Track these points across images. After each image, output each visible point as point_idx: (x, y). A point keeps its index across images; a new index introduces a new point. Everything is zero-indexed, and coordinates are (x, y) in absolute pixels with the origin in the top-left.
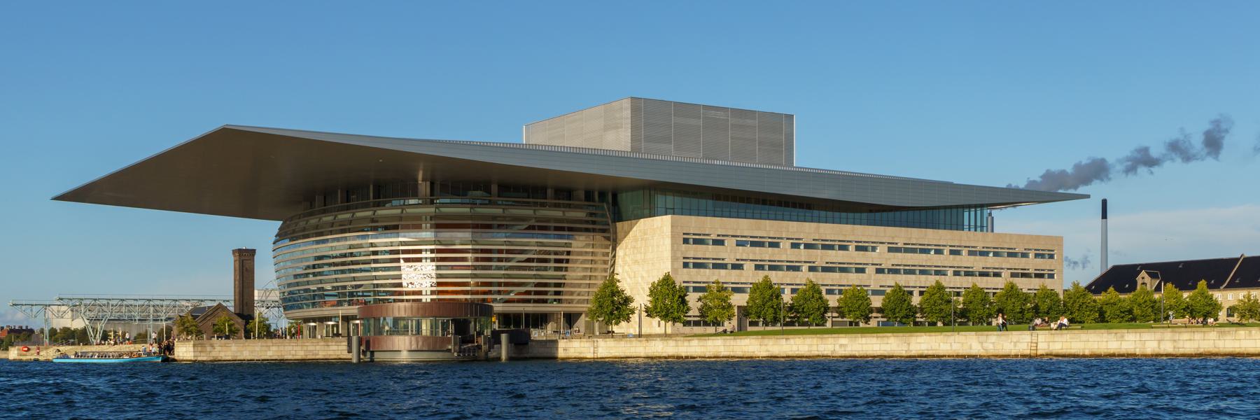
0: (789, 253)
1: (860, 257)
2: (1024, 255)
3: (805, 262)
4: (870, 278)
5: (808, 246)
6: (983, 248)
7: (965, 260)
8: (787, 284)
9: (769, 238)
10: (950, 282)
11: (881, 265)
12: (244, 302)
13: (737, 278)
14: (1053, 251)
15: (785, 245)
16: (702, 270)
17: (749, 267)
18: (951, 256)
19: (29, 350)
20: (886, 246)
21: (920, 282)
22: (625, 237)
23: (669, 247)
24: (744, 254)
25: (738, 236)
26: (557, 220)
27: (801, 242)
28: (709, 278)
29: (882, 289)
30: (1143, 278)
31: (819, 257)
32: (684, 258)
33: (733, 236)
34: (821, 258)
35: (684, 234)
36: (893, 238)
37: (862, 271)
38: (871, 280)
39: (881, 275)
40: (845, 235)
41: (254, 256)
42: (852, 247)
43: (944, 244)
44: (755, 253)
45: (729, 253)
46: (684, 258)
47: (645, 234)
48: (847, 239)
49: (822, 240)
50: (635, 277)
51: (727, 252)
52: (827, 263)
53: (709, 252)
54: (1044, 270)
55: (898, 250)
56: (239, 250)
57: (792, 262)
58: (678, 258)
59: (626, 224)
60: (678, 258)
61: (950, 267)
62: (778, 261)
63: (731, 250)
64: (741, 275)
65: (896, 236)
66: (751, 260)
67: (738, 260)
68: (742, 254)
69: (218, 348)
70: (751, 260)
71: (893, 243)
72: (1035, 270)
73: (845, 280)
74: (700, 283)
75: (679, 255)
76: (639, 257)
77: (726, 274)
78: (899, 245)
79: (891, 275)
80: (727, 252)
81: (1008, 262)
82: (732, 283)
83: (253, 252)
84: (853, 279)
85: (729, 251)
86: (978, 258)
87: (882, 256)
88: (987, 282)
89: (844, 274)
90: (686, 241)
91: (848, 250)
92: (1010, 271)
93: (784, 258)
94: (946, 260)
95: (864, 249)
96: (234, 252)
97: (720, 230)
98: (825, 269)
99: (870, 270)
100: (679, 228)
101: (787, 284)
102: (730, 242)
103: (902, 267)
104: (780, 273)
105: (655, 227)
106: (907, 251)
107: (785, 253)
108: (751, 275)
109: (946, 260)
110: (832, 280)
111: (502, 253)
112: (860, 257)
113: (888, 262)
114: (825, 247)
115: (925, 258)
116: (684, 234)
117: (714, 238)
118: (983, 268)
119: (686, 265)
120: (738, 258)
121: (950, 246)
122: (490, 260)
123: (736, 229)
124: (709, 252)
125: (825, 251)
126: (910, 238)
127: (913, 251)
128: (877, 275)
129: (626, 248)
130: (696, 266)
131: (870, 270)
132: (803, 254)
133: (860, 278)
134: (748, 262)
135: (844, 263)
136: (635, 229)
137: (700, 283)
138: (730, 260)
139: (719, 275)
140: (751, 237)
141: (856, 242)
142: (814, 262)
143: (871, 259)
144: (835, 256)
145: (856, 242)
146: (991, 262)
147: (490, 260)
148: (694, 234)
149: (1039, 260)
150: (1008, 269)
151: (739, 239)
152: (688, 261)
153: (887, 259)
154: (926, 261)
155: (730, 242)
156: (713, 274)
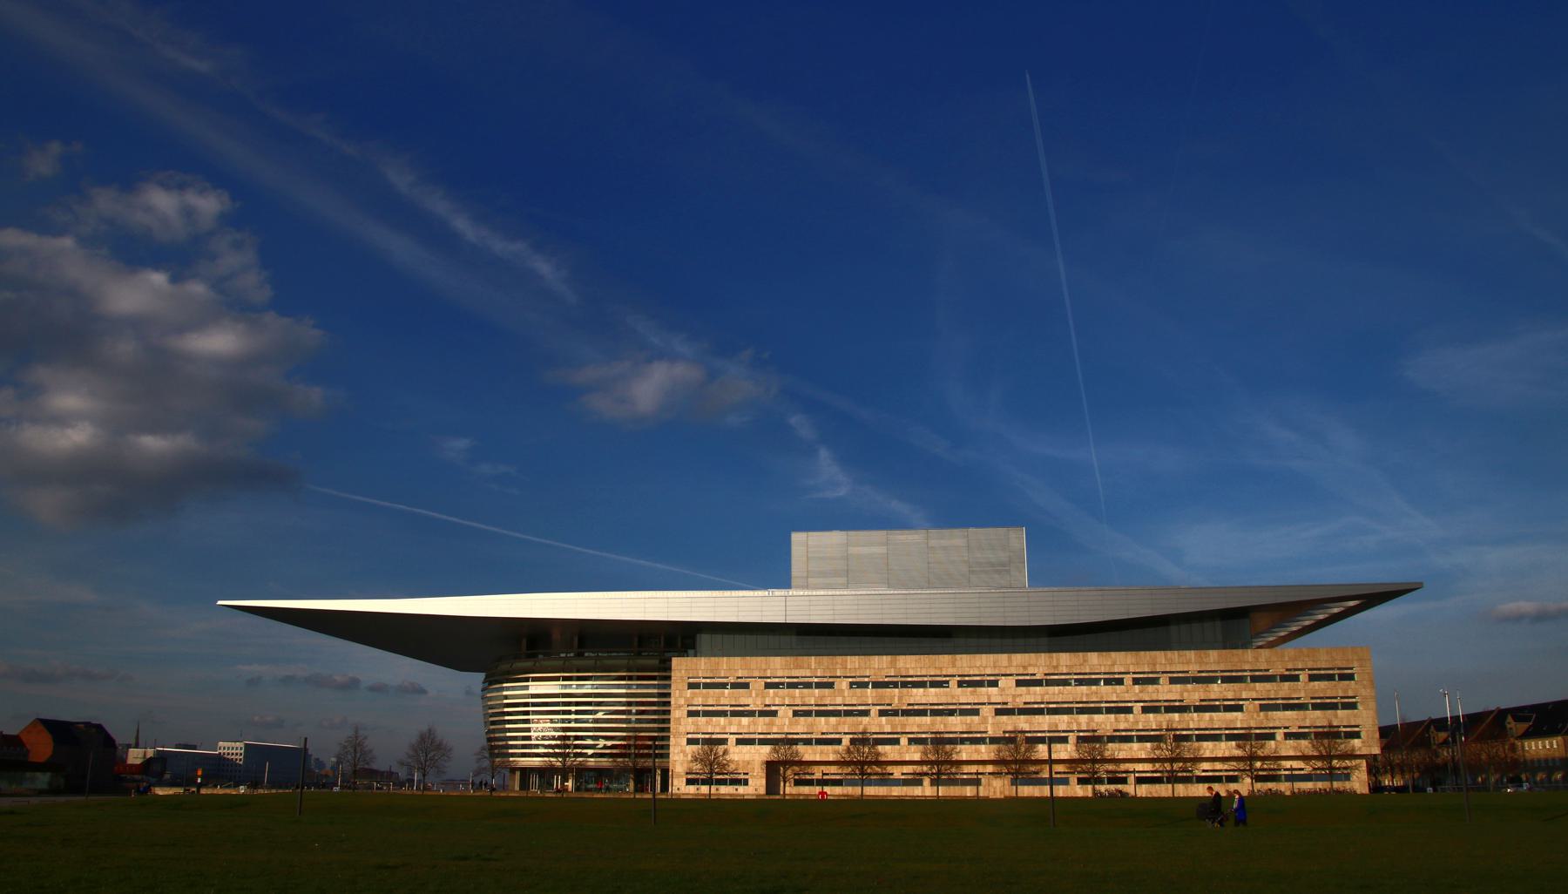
0: (846, 694)
1: (965, 696)
2: (1284, 678)
4: (985, 721)
5: (877, 685)
6: (1199, 672)
7: (1165, 692)
10: (1137, 722)
11: (1006, 703)
13: (765, 727)
14: (1352, 669)
15: (844, 684)
16: (714, 719)
17: (785, 714)
18: (1137, 686)
20: (1011, 681)
21: (1079, 724)
24: (777, 699)
25: (769, 678)
27: (866, 680)
28: (725, 728)
31: (896, 701)
34: (895, 697)
36: (1025, 668)
37: (976, 712)
38: (993, 725)
40: (941, 669)
42: (953, 682)
44: (794, 697)
45: (752, 700)
48: (944, 673)
49: (902, 676)
51: (751, 696)
52: (909, 705)
53: (727, 697)
54: (1336, 698)
55: (1038, 683)
57: (855, 705)
58: (680, 706)
60: (680, 706)
61: (1136, 702)
62: (831, 705)
63: (757, 695)
64: (772, 724)
65: (1030, 665)
66: (788, 705)
67: (766, 705)
68: (774, 698)
70: (788, 705)
71: (1027, 675)
72: (1312, 698)
73: (942, 726)
75: (682, 701)
77: (749, 723)
80: (751, 696)
81: (1254, 689)
84: (956, 724)
85: (754, 695)
86: (1189, 686)
87: (1007, 692)
88: (1211, 719)
89: (939, 718)
90: (692, 686)
92: (1257, 702)
93: (839, 700)
94: (1127, 692)
95: (980, 684)
97: (740, 671)
98: (906, 713)
99: (987, 711)
100: (683, 671)
103: (1042, 706)
104: (833, 720)
106: (1050, 683)
107: (843, 695)
108: (787, 723)
109: (1127, 692)
110: (919, 726)
112: (965, 696)
113: (1018, 700)
114: (905, 685)
115: (1085, 692)
117: (732, 681)
118: (1201, 700)
119: (691, 714)
120: (767, 703)
121: (1134, 673)
122: (569, 712)
123: (765, 670)
124: (727, 697)
125: (905, 690)
126: (1056, 667)
127: (1065, 683)
128: (998, 717)
130: (707, 714)
131: (987, 711)
133: (968, 722)
139: (740, 724)
141: (959, 676)
142: (888, 705)
143: (986, 697)
144: (919, 696)
145: (959, 676)
146: (1217, 691)
147: (569, 712)
149: (1317, 685)
150: (1253, 699)
151: (769, 680)
152: (694, 708)
153: (1014, 696)
154: (1087, 695)
156: (730, 724)
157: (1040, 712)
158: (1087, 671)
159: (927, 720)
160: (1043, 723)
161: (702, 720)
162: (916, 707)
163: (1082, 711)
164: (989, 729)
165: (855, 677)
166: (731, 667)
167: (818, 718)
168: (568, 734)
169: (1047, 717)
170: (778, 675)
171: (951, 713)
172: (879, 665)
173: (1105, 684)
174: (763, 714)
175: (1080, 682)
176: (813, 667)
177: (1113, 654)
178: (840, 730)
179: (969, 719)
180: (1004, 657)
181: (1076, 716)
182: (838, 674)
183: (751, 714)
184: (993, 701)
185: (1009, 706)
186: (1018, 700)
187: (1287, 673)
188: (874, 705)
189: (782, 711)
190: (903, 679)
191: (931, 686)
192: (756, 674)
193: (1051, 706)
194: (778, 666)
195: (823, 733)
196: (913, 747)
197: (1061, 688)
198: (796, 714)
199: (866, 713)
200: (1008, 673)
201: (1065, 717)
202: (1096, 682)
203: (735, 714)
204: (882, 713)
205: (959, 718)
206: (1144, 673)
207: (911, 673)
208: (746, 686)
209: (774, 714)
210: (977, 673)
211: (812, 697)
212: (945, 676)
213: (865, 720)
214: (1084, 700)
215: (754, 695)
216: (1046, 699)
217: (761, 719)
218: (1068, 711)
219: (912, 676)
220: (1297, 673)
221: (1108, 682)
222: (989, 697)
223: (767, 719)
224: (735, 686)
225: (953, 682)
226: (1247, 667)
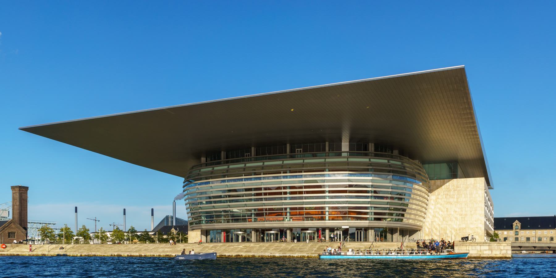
12: (22, 219)
19: (6, 246)
22: (437, 188)
30: (516, 224)
41: (27, 191)
47: (457, 187)
50: (447, 211)
56: (19, 186)
59: (438, 182)
76: (451, 200)
83: (27, 188)
96: (13, 188)
105: (468, 183)
111: (262, 195)
129: (439, 195)
136: (448, 184)
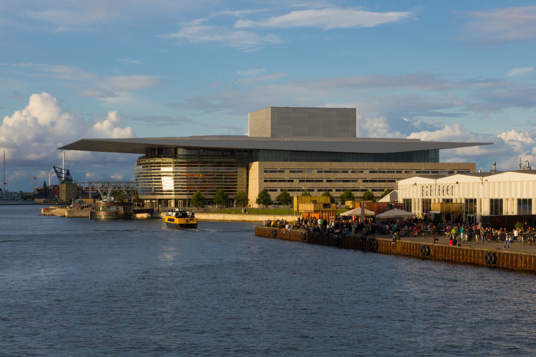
0: (316, 174)
3: (325, 178)
5: (326, 172)
6: (425, 169)
8: (316, 188)
9: (306, 169)
16: (273, 183)
17: (296, 181)
18: (406, 174)
20: (368, 171)
21: (388, 185)
23: (258, 174)
26: (225, 163)
27: (322, 170)
29: (366, 189)
31: (332, 177)
32: (265, 178)
33: (288, 169)
34: (332, 176)
35: (265, 169)
36: (372, 167)
37: (356, 181)
38: (361, 185)
39: (365, 183)
42: (350, 171)
43: (402, 168)
45: (286, 176)
46: (265, 178)
48: (347, 168)
49: (334, 169)
53: (277, 176)
55: (376, 172)
69: (75, 213)
74: (273, 188)
75: (262, 177)
78: (376, 170)
79: (371, 183)
82: (288, 188)
85: (286, 175)
89: (345, 183)
90: (265, 172)
91: (348, 173)
93: (314, 177)
99: (360, 181)
101: (316, 188)
102: (287, 172)
104: (312, 183)
107: (315, 175)
114: (335, 172)
116: (265, 169)
119: (265, 181)
123: (290, 166)
124: (277, 176)
127: (384, 172)
132: (324, 175)
134: (296, 179)
135: (346, 178)
137: (273, 188)
138: (287, 178)
140: (297, 169)
141: (352, 169)
142: (330, 178)
145: (352, 169)
148: (269, 169)
151: (291, 170)
153: (369, 176)
155: (287, 172)
157: (376, 181)
158: (391, 168)
159: (342, 183)
160: (377, 185)
161: (269, 183)
162: (338, 179)
163: (389, 181)
164: (361, 187)
165: (318, 169)
166: (278, 165)
167: (307, 183)
168: (214, 186)
169: (379, 183)
170: (294, 168)
171: (348, 181)
172: (327, 165)
173: (396, 173)
174: (289, 181)
175: (388, 172)
176: (305, 165)
177: (399, 163)
178: (314, 187)
179: (354, 183)
180: (366, 163)
181: (387, 183)
182: (314, 168)
183: (285, 181)
184: (362, 177)
185: (367, 179)
186: (370, 177)
187: (451, 171)
188: (325, 178)
189: (295, 180)
190: (334, 170)
191: (343, 173)
192: (287, 168)
193: (380, 179)
194: (294, 165)
195: (309, 188)
196: (337, 192)
197: (383, 174)
198: (300, 181)
199: (322, 181)
200: (367, 168)
201: (384, 183)
202: (393, 172)
203: (280, 181)
204: (328, 181)
205: (351, 183)
206: (408, 169)
207: (337, 168)
208: (283, 172)
209: (292, 181)
210: (357, 168)
211: (305, 176)
212: (347, 169)
213: (322, 183)
214: (390, 178)
215: (286, 175)
216: (378, 177)
217: (289, 183)
218: (385, 181)
219: (337, 169)
220: (454, 170)
221: (397, 172)
222: (361, 176)
223: (291, 183)
224: (280, 172)
225: (350, 171)
226: (439, 168)
